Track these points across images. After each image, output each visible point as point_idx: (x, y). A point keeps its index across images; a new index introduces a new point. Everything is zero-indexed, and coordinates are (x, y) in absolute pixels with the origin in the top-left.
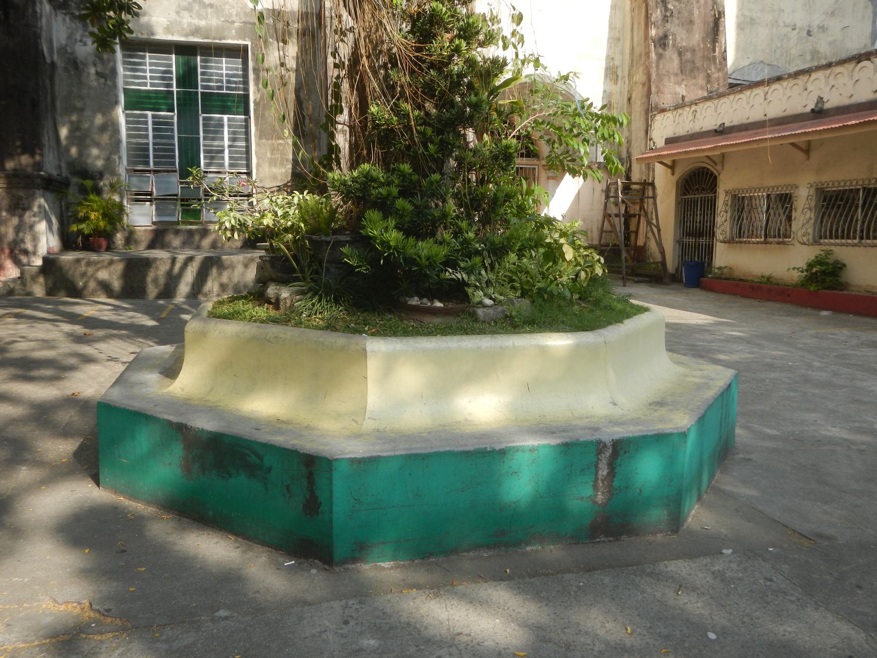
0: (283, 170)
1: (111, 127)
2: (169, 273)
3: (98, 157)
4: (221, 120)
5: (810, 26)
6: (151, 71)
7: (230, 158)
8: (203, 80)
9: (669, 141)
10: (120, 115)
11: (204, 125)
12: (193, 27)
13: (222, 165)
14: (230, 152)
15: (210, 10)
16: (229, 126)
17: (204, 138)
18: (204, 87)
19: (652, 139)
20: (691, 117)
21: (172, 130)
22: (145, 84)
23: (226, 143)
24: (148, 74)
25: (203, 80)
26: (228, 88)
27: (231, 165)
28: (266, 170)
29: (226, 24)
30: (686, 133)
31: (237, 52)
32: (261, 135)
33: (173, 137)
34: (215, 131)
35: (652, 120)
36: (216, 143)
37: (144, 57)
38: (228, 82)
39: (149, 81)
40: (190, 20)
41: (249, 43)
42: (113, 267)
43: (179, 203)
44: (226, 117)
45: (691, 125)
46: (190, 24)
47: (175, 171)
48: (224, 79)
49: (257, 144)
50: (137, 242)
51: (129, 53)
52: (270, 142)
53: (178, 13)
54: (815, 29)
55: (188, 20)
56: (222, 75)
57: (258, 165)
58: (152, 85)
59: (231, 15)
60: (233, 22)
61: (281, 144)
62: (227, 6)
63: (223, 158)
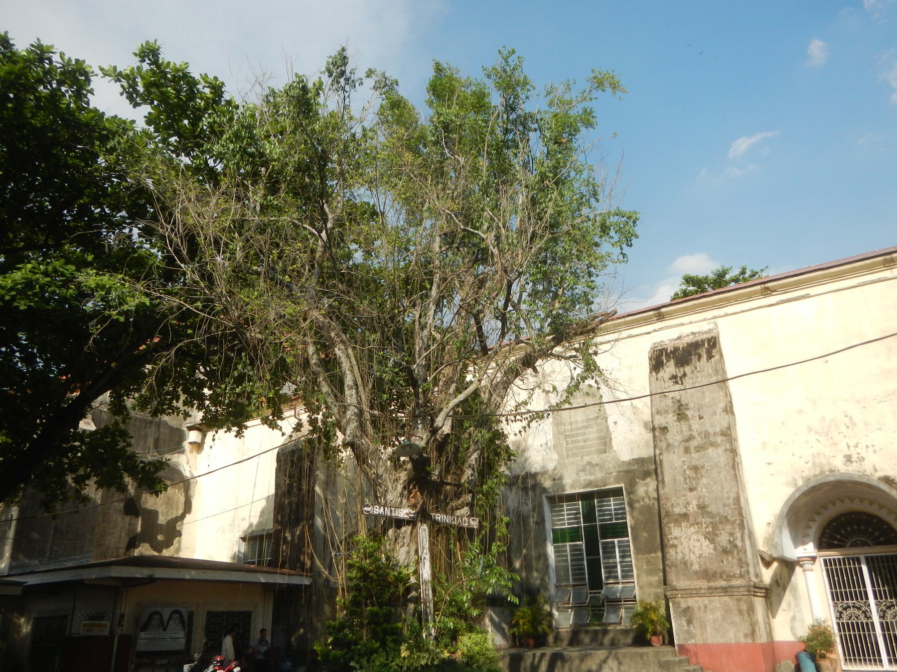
0: (657, 578)
1: (544, 556)
2: (532, 664)
3: (537, 578)
4: (613, 543)
6: (568, 515)
7: (622, 571)
8: (599, 516)
10: (550, 549)
11: (603, 548)
12: (587, 482)
13: (617, 577)
14: (622, 567)
15: (597, 468)
16: (619, 547)
17: (604, 558)
18: (601, 521)
21: (582, 554)
22: (564, 524)
23: (618, 559)
24: (566, 517)
25: (599, 516)
26: (616, 519)
27: (623, 577)
28: (645, 579)
29: (607, 475)
31: (617, 492)
32: (638, 551)
33: (582, 560)
34: (609, 550)
36: (611, 561)
37: (563, 506)
38: (616, 514)
39: (566, 522)
40: (585, 477)
41: (622, 485)
42: (505, 659)
43: (590, 609)
44: (616, 540)
46: (585, 480)
47: (586, 585)
48: (613, 512)
49: (636, 559)
50: (561, 640)
51: (607, 487)
52: (645, 556)
53: (577, 474)
55: (584, 478)
56: (611, 510)
57: (638, 576)
58: (569, 524)
59: (610, 468)
60: (611, 473)
61: (653, 557)
62: (607, 463)
63: (617, 572)
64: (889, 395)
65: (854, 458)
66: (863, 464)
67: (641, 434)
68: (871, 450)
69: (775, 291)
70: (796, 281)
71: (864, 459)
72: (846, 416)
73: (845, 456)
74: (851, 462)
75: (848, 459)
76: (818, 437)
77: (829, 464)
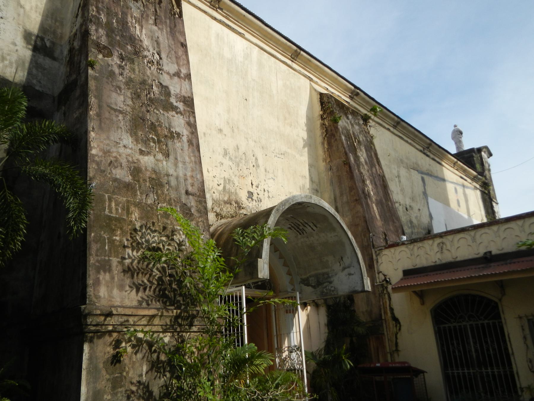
5: (406, 205)
9: (407, 273)
19: (381, 272)
20: (436, 248)
30: (433, 264)
35: (377, 256)
45: (439, 256)
54: (408, 207)
64: (281, 154)
65: (255, 197)
66: (260, 205)
67: (15, 44)
68: (266, 193)
69: (221, 9)
70: (241, 14)
71: (261, 201)
72: (254, 156)
73: (249, 192)
74: (252, 200)
75: (250, 194)
76: (231, 163)
77: (236, 194)
